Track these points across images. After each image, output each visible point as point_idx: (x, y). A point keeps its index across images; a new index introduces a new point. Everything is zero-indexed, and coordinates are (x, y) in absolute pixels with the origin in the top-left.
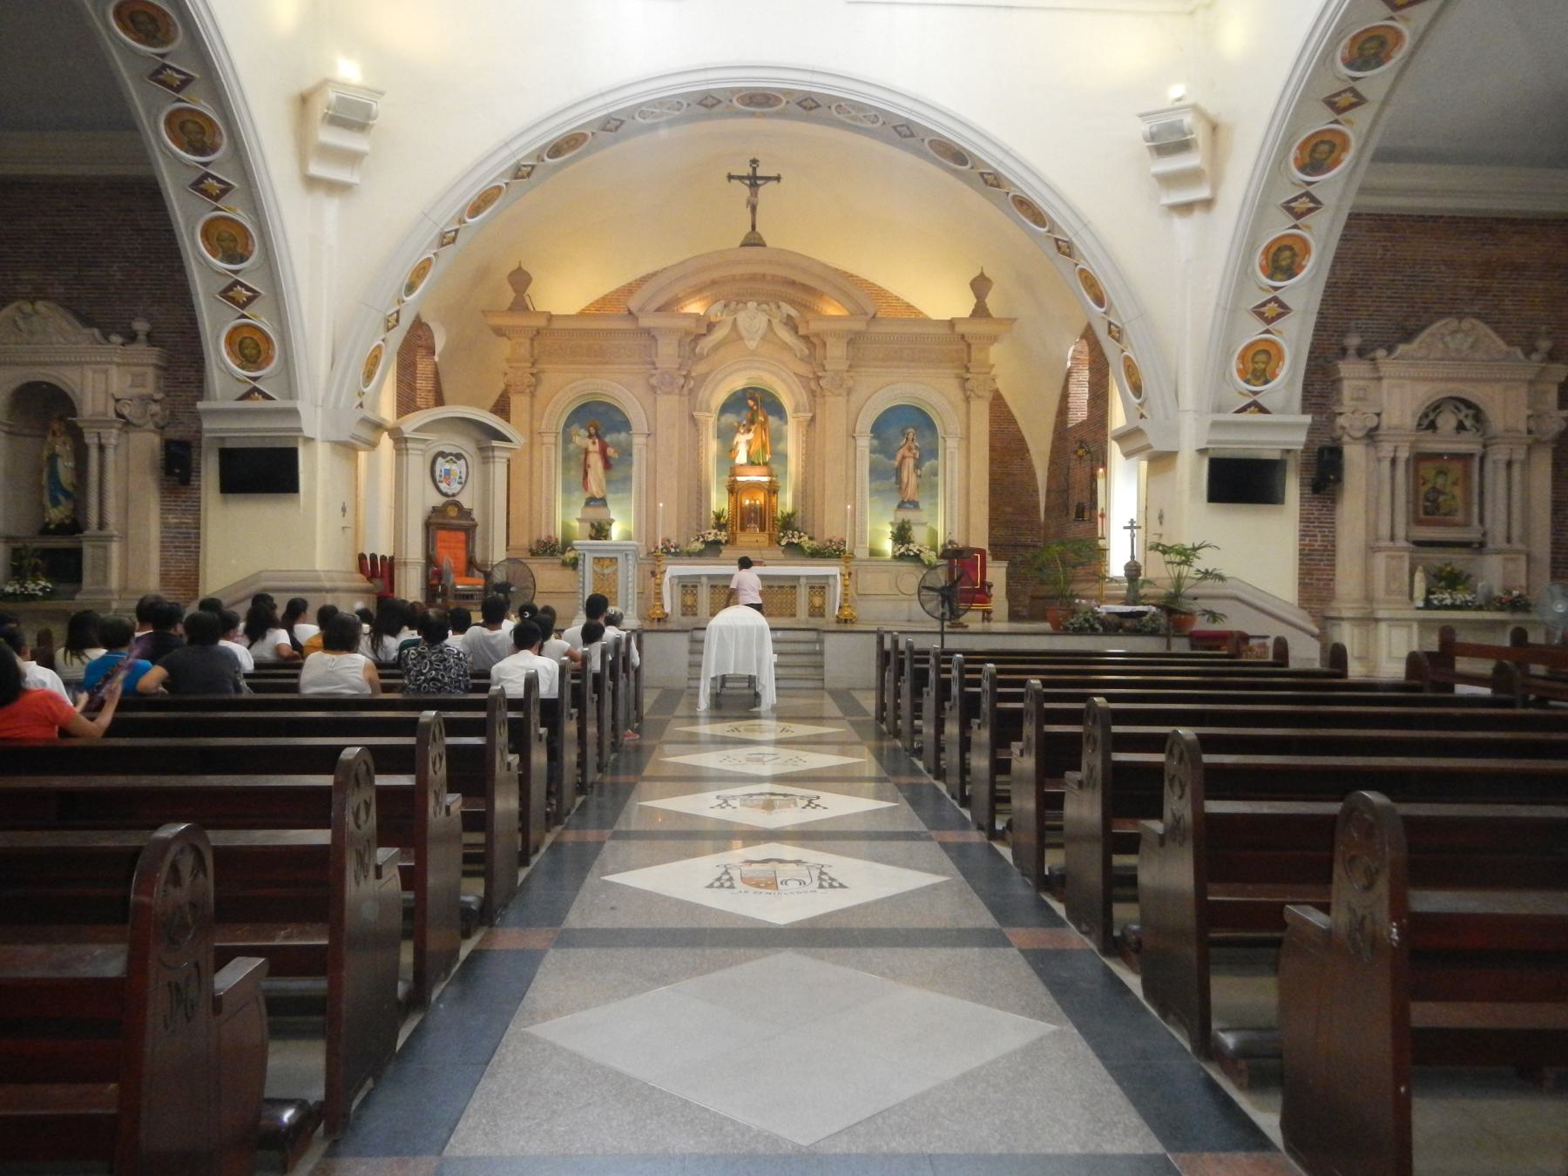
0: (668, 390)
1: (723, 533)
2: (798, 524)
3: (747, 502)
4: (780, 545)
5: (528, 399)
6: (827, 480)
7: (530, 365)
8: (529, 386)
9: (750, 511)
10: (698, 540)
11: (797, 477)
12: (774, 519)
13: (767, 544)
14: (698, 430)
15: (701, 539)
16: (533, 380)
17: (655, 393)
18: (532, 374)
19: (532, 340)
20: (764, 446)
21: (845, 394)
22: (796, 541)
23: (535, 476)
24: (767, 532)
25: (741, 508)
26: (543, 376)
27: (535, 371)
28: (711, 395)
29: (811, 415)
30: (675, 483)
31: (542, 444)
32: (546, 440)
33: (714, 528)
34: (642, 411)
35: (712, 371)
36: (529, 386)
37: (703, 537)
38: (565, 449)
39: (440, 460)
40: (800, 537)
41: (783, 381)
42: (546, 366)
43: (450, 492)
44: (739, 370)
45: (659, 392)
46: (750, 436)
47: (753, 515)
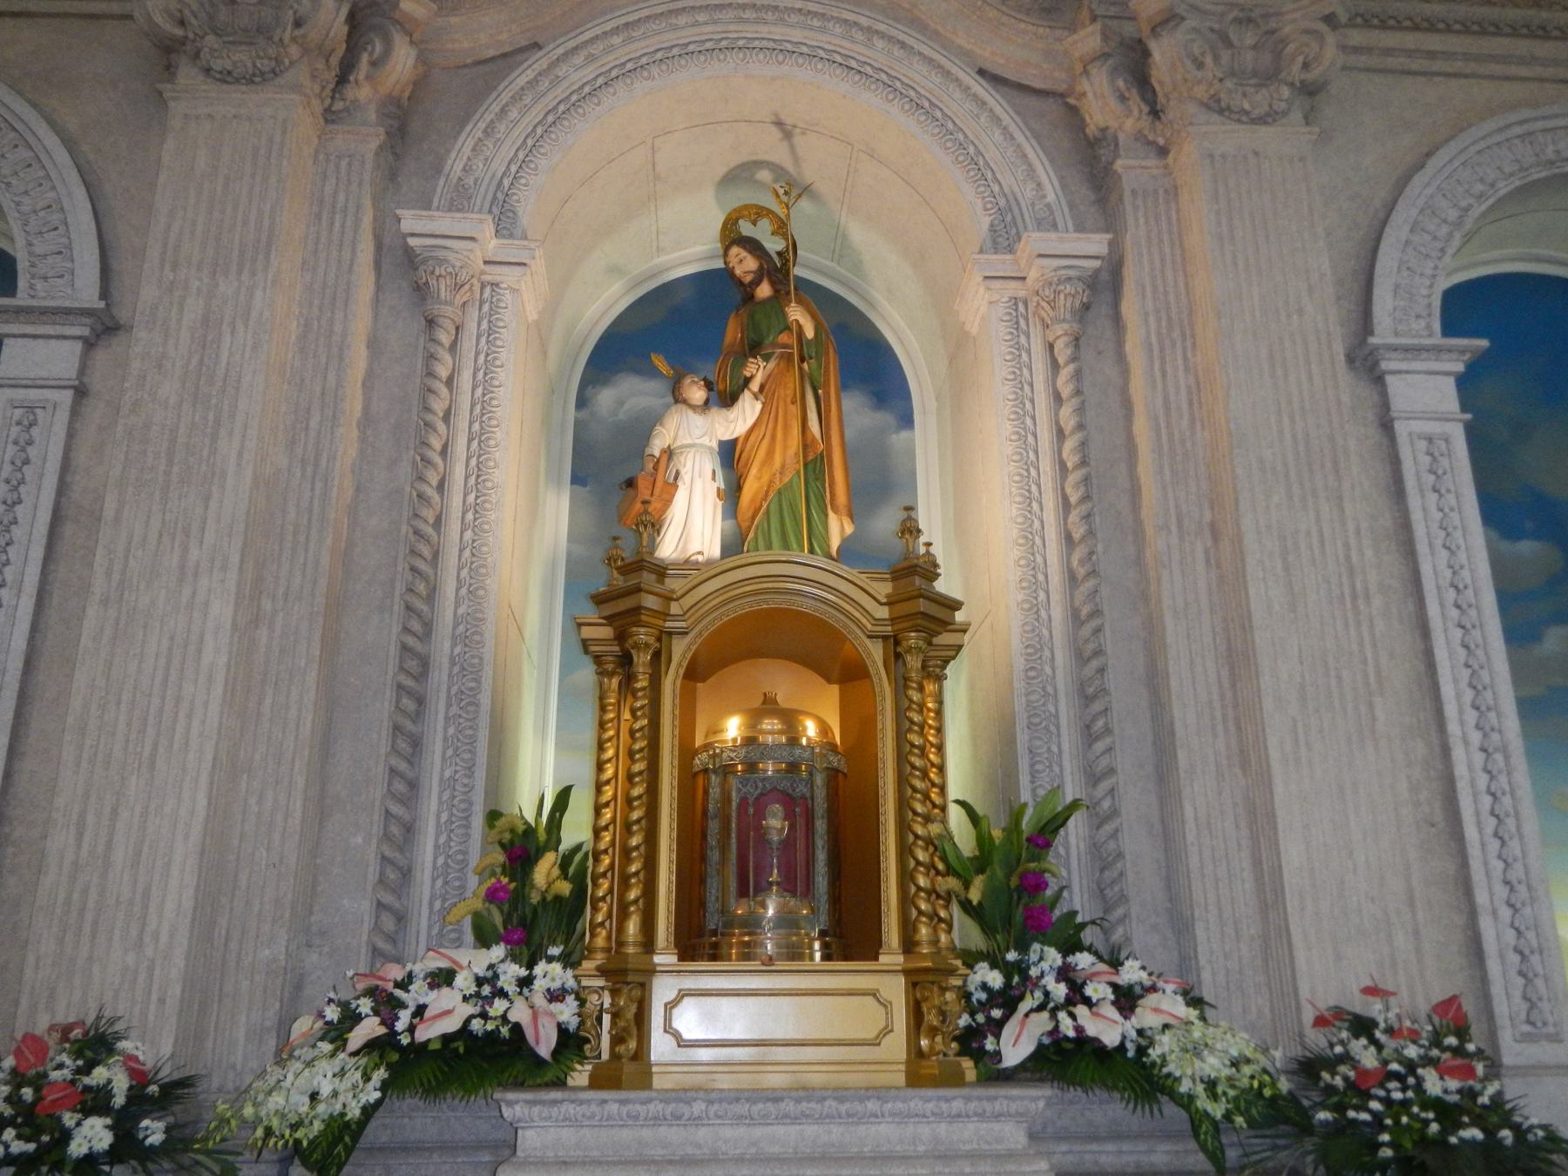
0: (242, 58)
1: (550, 973)
2: (1079, 901)
3: (733, 728)
4: (995, 1075)
6: (1264, 593)
9: (753, 810)
10: (336, 1034)
11: (1035, 610)
12: (940, 845)
13: (901, 1079)
14: (431, 323)
15: (370, 1028)
17: (170, 70)
20: (815, 465)
21: (1296, 116)
22: (1108, 1028)
24: (891, 957)
25: (690, 778)
28: (524, 160)
29: (1097, 244)
30: (222, 610)
33: (484, 939)
34: (80, 194)
35: (536, 46)
37: (387, 1005)
40: (1126, 999)
41: (920, 106)
44: (687, 52)
45: (187, 74)
46: (742, 417)
47: (775, 823)
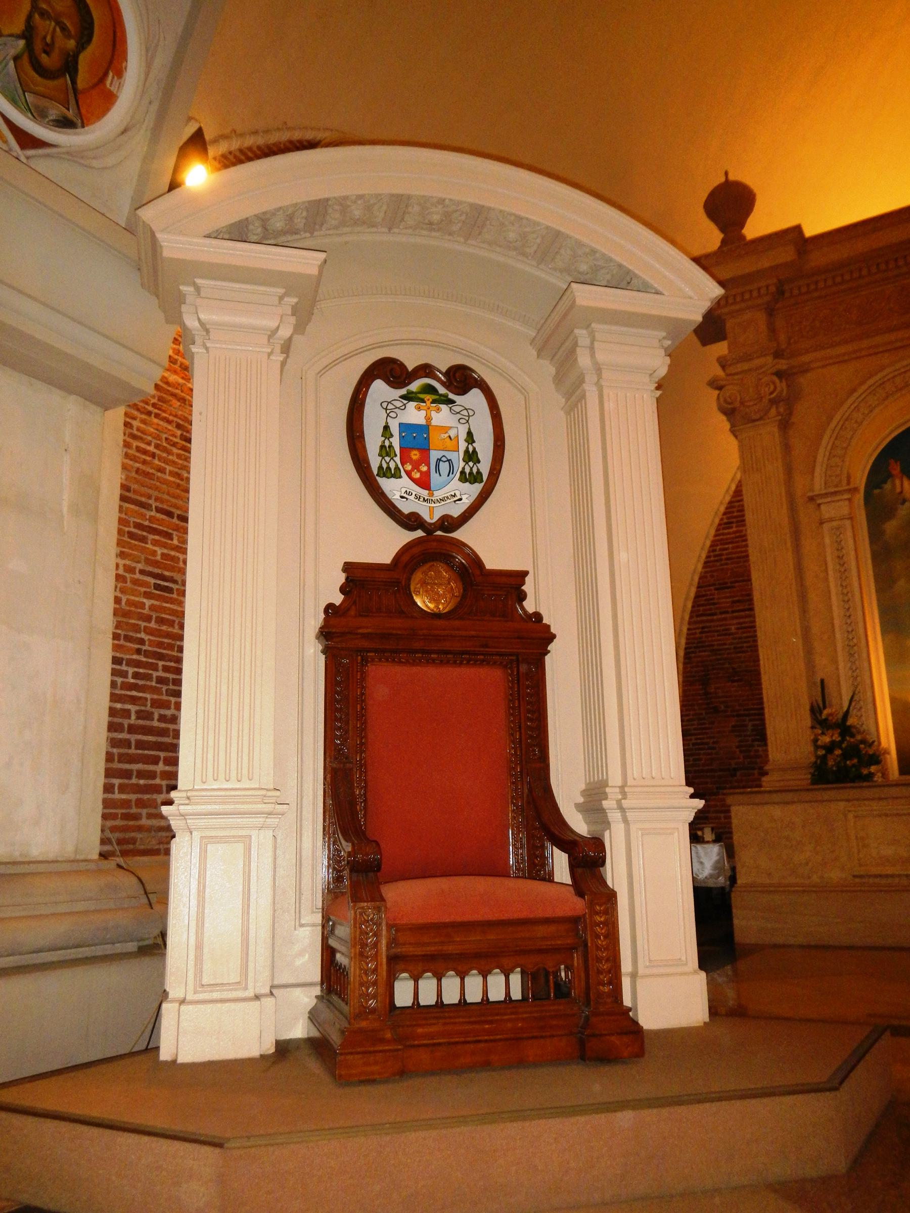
5: (776, 430)
7: (770, 359)
8: (773, 402)
16: (781, 386)
18: (779, 374)
19: (770, 312)
23: (813, 597)
26: (804, 381)
27: (783, 365)
31: (822, 523)
32: (827, 511)
36: (773, 402)
38: (875, 534)
39: (379, 390)
42: (806, 358)
43: (430, 513)
